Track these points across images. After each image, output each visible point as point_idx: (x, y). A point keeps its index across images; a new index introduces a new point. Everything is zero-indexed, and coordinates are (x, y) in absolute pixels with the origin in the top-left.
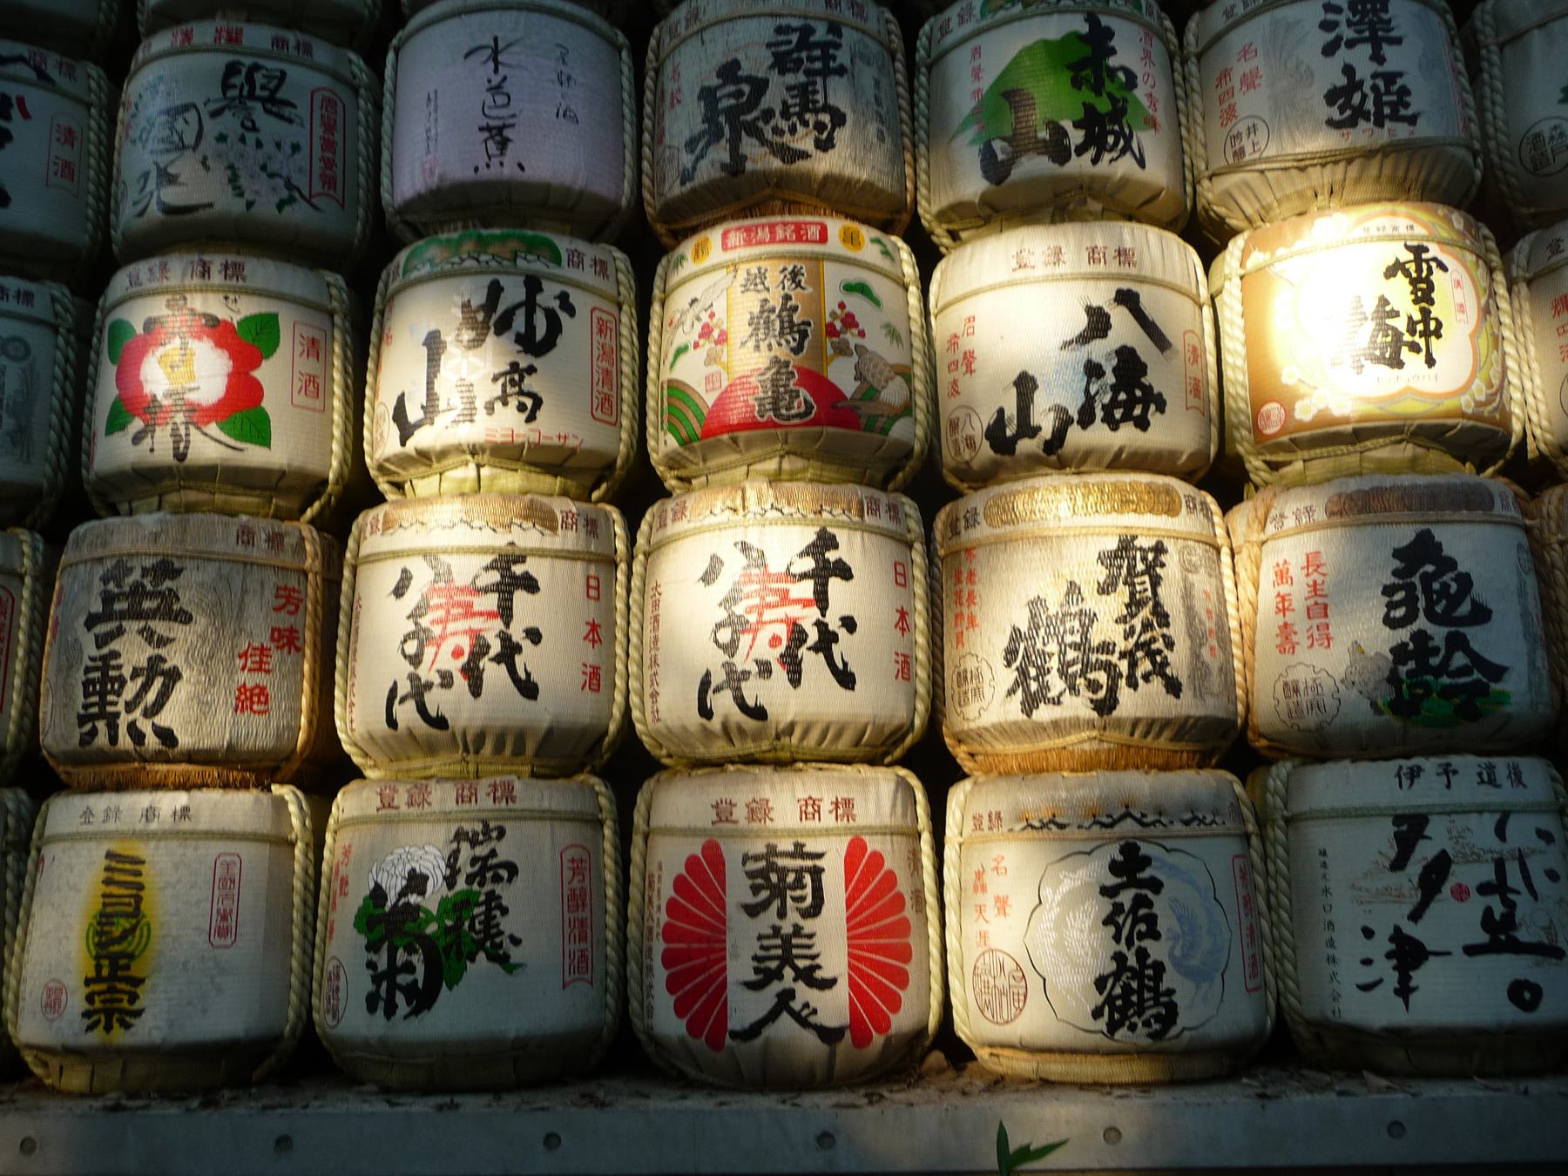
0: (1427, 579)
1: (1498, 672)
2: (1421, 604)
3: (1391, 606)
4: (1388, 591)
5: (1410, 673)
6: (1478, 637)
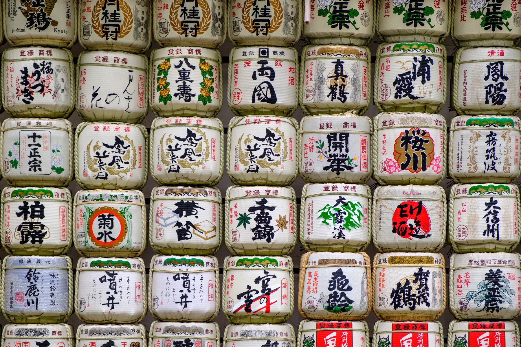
0: (339, 280)
1: (351, 302)
2: (337, 286)
3: (330, 285)
4: (330, 282)
5: (332, 301)
6: (348, 294)
